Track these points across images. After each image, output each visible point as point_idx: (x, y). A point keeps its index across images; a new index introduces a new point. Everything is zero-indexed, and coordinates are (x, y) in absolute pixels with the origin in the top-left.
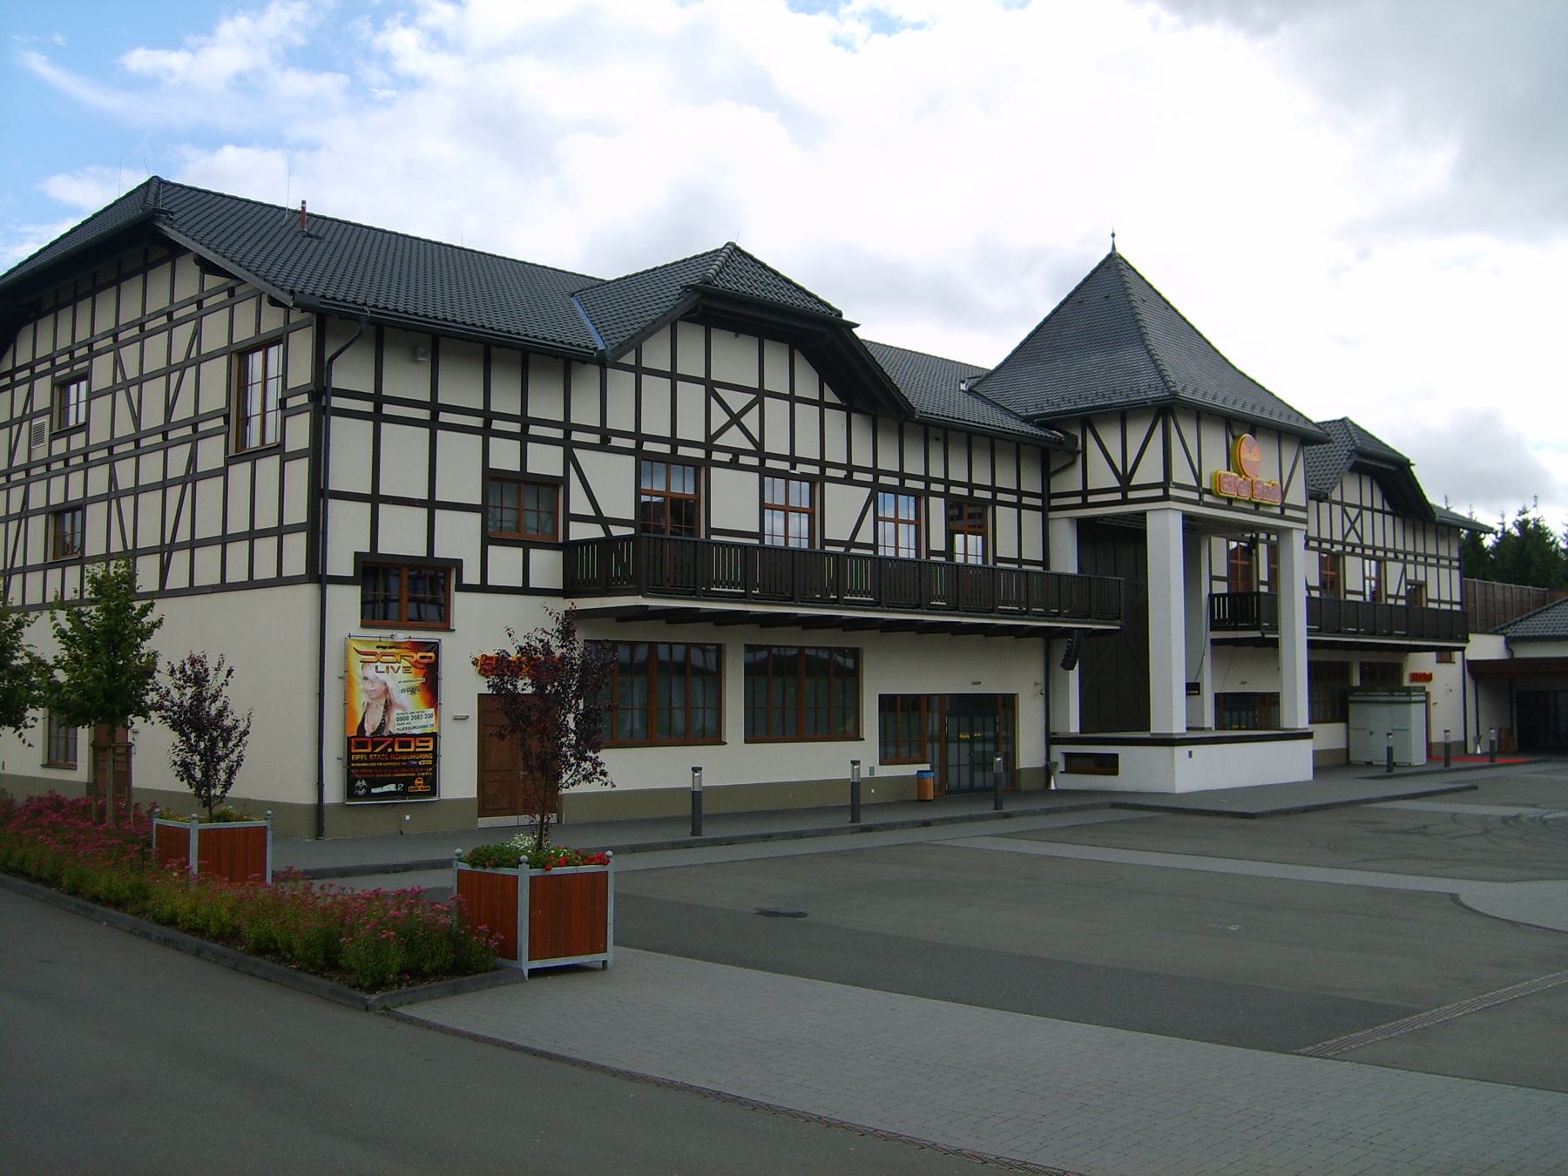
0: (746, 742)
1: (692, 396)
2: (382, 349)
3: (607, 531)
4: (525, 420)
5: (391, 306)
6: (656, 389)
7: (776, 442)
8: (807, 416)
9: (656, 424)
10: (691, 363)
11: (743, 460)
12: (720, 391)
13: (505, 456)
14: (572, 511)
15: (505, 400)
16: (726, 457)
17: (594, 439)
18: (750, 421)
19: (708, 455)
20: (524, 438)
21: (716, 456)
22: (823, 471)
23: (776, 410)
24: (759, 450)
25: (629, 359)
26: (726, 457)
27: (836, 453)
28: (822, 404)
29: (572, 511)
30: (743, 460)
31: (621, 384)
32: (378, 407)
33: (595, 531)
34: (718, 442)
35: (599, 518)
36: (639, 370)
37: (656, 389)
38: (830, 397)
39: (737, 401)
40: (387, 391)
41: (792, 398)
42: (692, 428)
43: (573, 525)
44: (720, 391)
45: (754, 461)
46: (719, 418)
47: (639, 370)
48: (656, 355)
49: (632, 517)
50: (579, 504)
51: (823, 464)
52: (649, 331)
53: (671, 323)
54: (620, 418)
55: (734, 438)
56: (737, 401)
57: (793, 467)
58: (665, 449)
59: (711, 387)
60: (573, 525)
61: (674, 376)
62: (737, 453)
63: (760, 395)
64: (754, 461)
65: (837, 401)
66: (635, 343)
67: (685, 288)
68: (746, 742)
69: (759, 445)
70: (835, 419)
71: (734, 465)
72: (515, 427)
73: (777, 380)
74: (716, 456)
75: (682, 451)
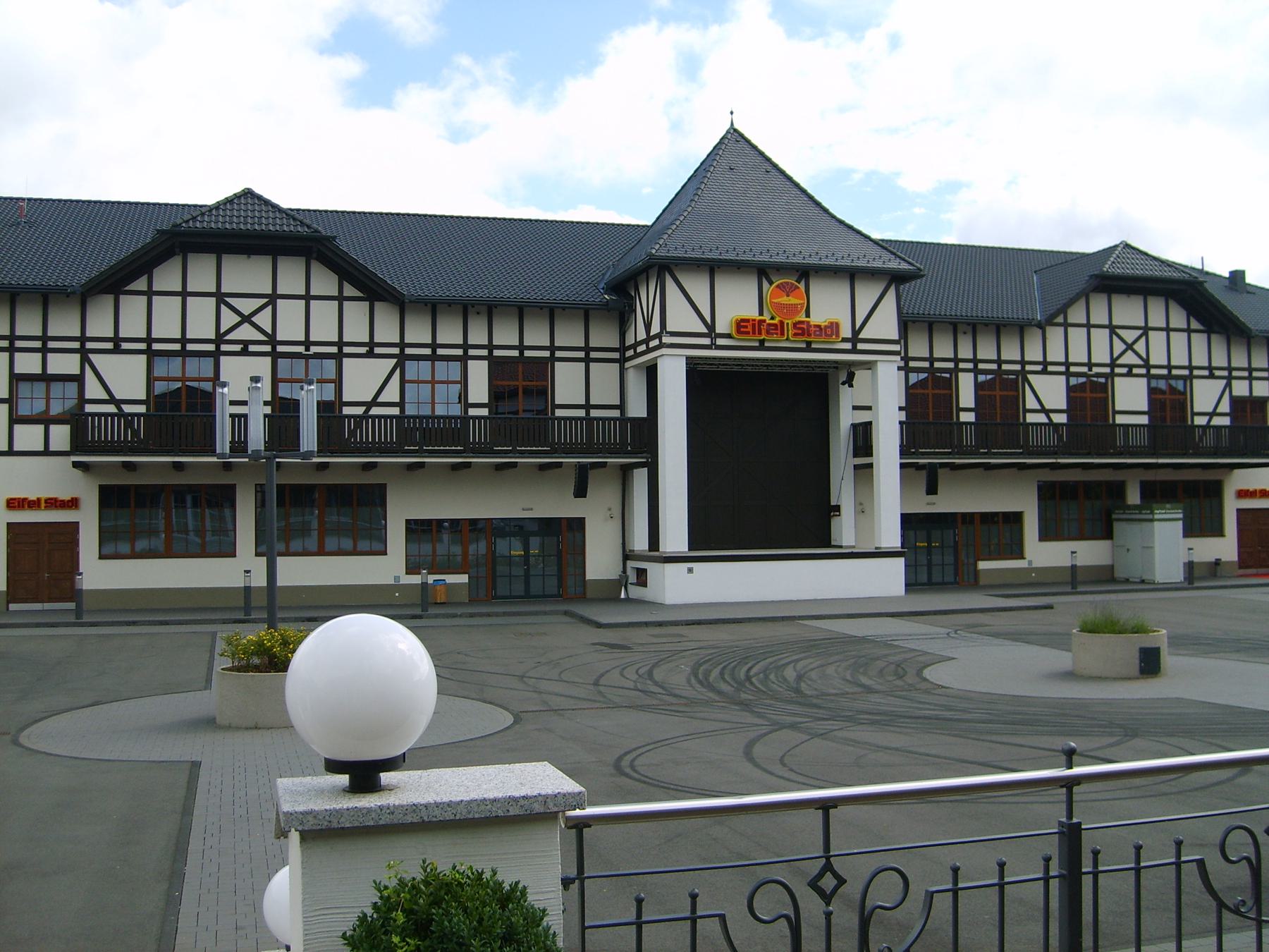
0: (1041, 540)
1: (1101, 337)
2: (932, 334)
3: (1049, 418)
4: (1250, 370)
5: (974, 315)
6: (1077, 336)
7: (1158, 357)
8: (1179, 340)
9: (1078, 355)
10: (1099, 316)
11: (1135, 371)
12: (1118, 331)
13: (1240, 389)
14: (961, 406)
15: (1239, 360)
16: (1124, 370)
17: (1206, 373)
18: (1140, 347)
19: (1112, 370)
20: (1250, 378)
21: (1117, 370)
22: (1191, 372)
23: (1157, 339)
24: (1147, 364)
25: (1060, 319)
26: (1124, 370)
27: (1200, 359)
28: (1189, 331)
29: (961, 406)
30: (1135, 371)
31: (1055, 335)
32: (1250, 374)
33: (1042, 418)
34: (1119, 362)
35: (1043, 410)
36: (1066, 325)
37: (1077, 336)
38: (1195, 325)
39: (1130, 336)
40: (1253, 366)
41: (1168, 330)
42: (1100, 355)
43: (961, 414)
44: (1118, 331)
45: (1143, 371)
46: (1119, 347)
47: (1066, 325)
48: (1077, 314)
49: (973, 406)
50: (1031, 403)
51: (1191, 368)
52: (1072, 302)
53: (1085, 295)
54: (1056, 354)
55: (1129, 358)
56: (1130, 336)
57: (1090, 370)
58: (1165, 372)
59: (1112, 329)
60: (961, 414)
61: (1089, 326)
62: (1131, 367)
63: (1146, 330)
64: (1143, 371)
65: (1201, 327)
66: (1063, 310)
67: (1091, 277)
68: (1041, 540)
69: (1147, 361)
70: (1199, 341)
71: (1129, 374)
72: (1246, 374)
73: (1157, 319)
74: (1117, 370)
75: (1174, 372)
